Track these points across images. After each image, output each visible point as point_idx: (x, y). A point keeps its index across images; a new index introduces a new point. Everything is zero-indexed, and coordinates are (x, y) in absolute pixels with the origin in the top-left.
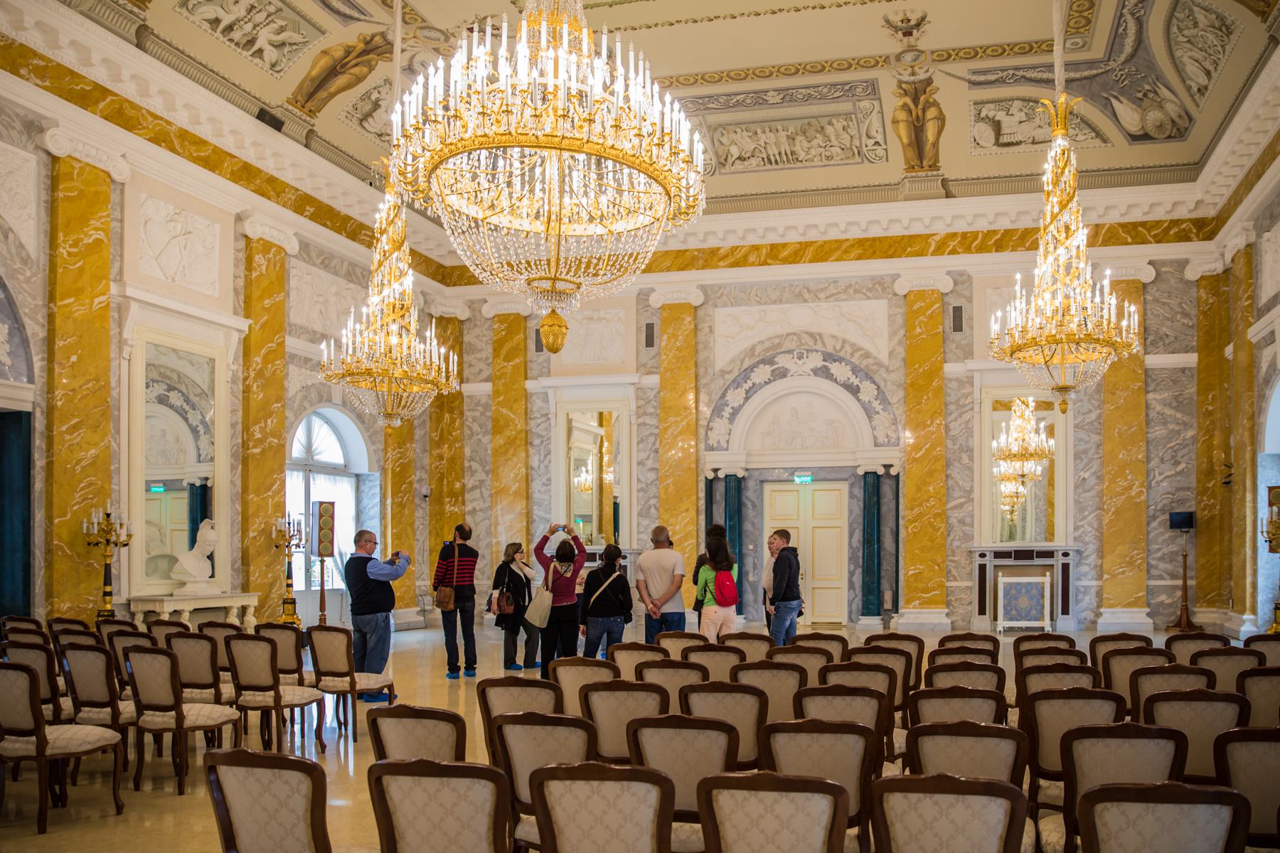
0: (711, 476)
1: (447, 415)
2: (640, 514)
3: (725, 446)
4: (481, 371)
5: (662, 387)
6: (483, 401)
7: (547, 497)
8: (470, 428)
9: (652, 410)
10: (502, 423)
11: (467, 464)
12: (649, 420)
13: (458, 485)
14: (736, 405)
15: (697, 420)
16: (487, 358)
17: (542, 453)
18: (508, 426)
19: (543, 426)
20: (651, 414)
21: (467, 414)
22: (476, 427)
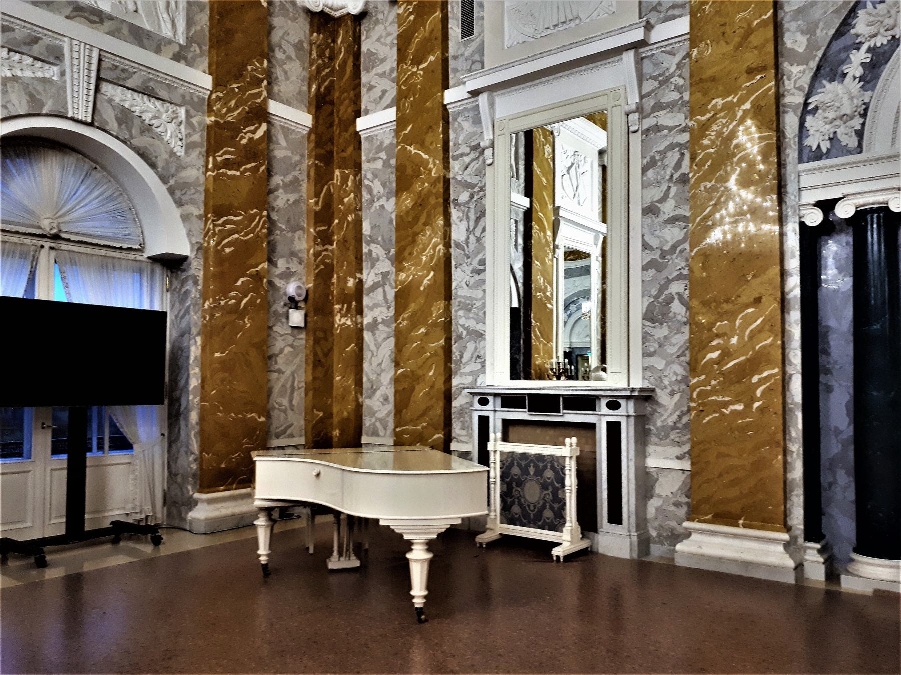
0: (815, 218)
1: (337, 173)
2: (649, 317)
3: (853, 143)
4: (384, 92)
5: (694, 38)
6: (387, 142)
7: (478, 294)
8: (370, 190)
9: (675, 96)
10: (409, 171)
11: (365, 250)
12: (666, 119)
13: (351, 283)
14: (881, 41)
15: (779, 97)
16: (392, 71)
17: (472, 216)
18: (418, 175)
19: (474, 166)
20: (671, 106)
21: (365, 166)
22: (377, 188)
